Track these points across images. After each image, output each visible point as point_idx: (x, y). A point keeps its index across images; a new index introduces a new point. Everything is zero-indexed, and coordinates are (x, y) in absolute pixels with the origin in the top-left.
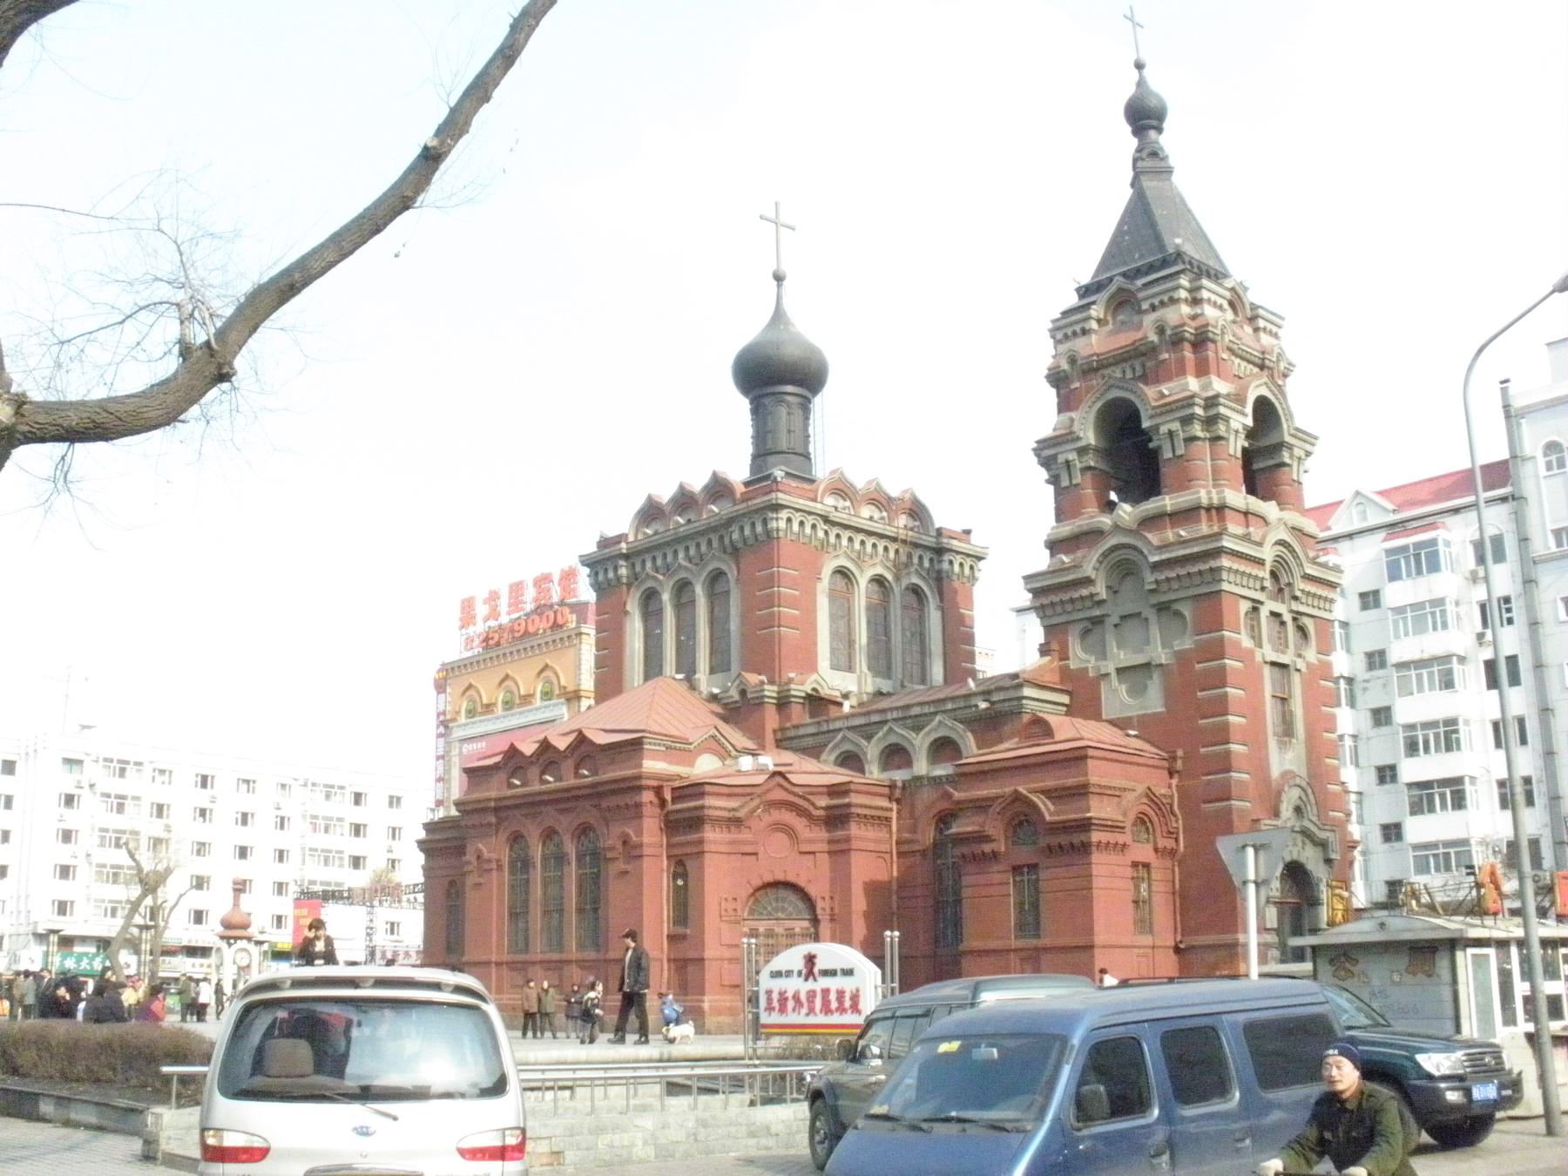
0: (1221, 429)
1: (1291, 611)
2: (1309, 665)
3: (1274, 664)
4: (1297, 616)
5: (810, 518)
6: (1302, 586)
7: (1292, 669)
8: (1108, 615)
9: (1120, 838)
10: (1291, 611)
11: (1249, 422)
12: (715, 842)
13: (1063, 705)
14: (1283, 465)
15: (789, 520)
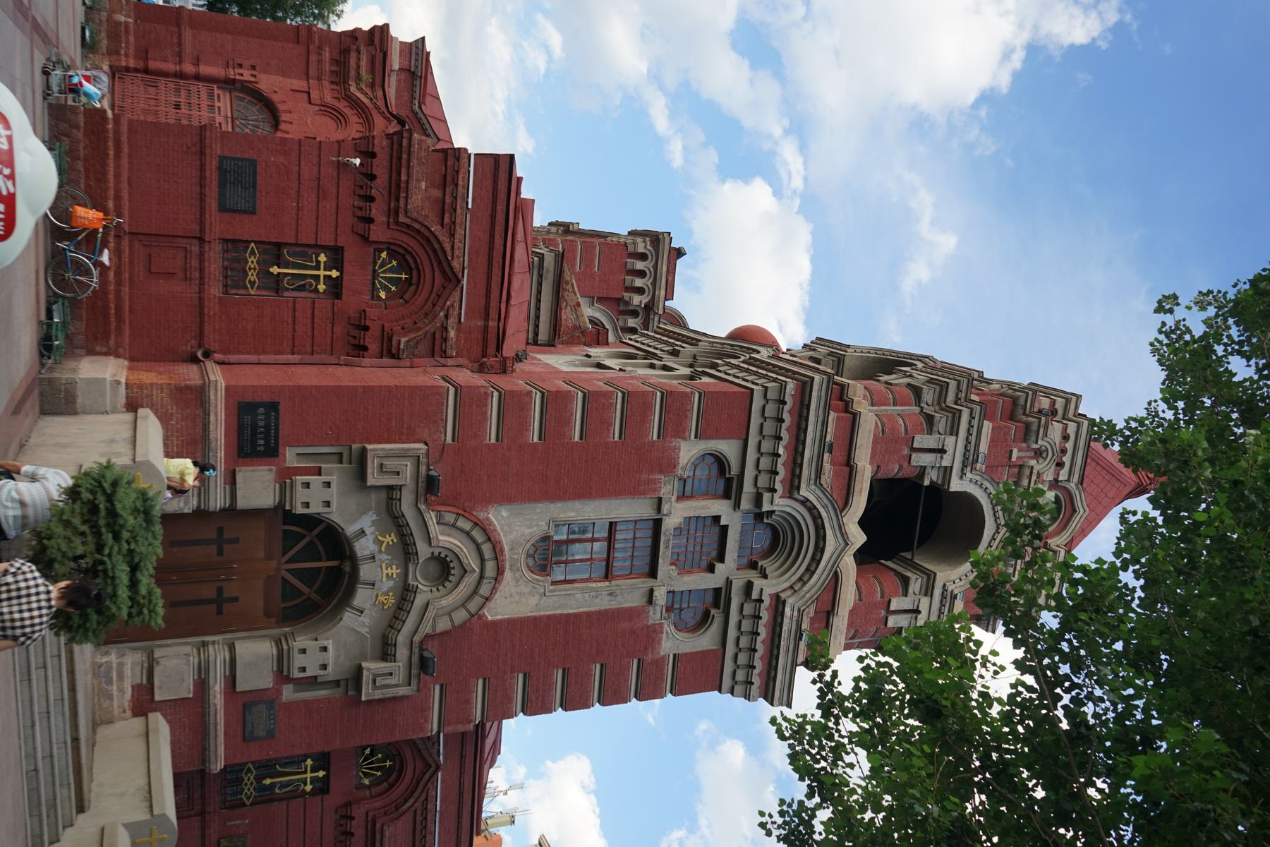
0: (942, 422)
1: (729, 583)
2: (655, 631)
3: (657, 523)
4: (720, 597)
5: (649, 283)
6: (766, 599)
7: (650, 583)
8: (660, 359)
9: (377, 211)
10: (729, 583)
11: (956, 485)
12: (319, 61)
13: (536, 334)
14: (905, 582)
15: (643, 257)
